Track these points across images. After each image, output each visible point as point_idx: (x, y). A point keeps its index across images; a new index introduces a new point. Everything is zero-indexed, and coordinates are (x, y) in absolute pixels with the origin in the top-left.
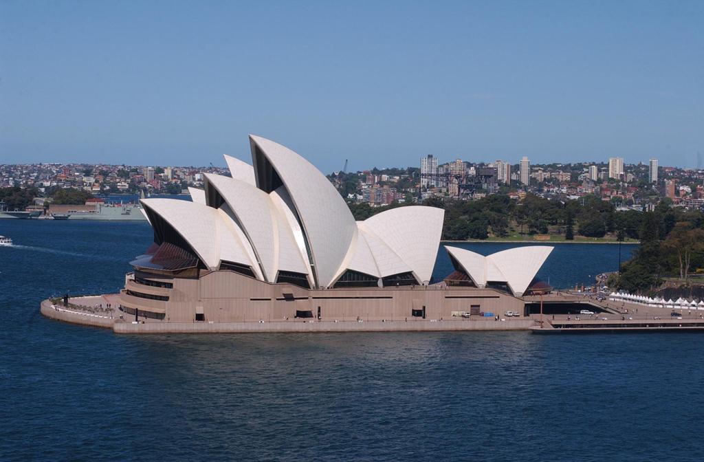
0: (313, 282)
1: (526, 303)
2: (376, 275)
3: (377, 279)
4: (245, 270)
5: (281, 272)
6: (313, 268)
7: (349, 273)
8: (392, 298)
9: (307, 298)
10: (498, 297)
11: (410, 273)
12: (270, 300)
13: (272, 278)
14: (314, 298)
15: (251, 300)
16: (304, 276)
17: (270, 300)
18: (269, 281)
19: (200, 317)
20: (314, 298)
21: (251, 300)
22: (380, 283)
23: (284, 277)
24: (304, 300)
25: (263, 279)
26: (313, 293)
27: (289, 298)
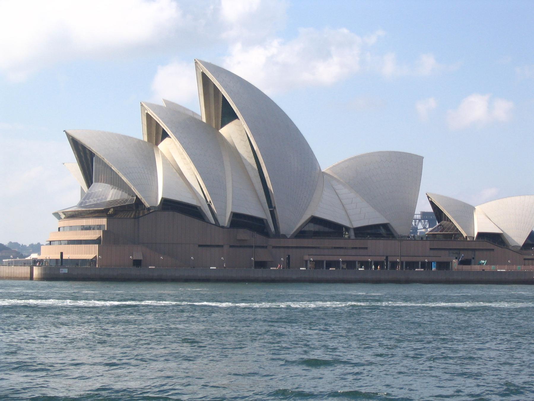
0: (273, 229)
2: (347, 224)
3: (347, 229)
4: (191, 211)
5: (235, 215)
6: (273, 214)
7: (314, 220)
8: (366, 248)
9: (266, 247)
10: (493, 250)
11: (386, 226)
12: (222, 246)
13: (225, 220)
14: (274, 247)
15: (200, 246)
18: (221, 224)
19: (137, 263)
21: (200, 246)
22: (352, 233)
23: (239, 220)
25: (213, 222)
26: (273, 242)
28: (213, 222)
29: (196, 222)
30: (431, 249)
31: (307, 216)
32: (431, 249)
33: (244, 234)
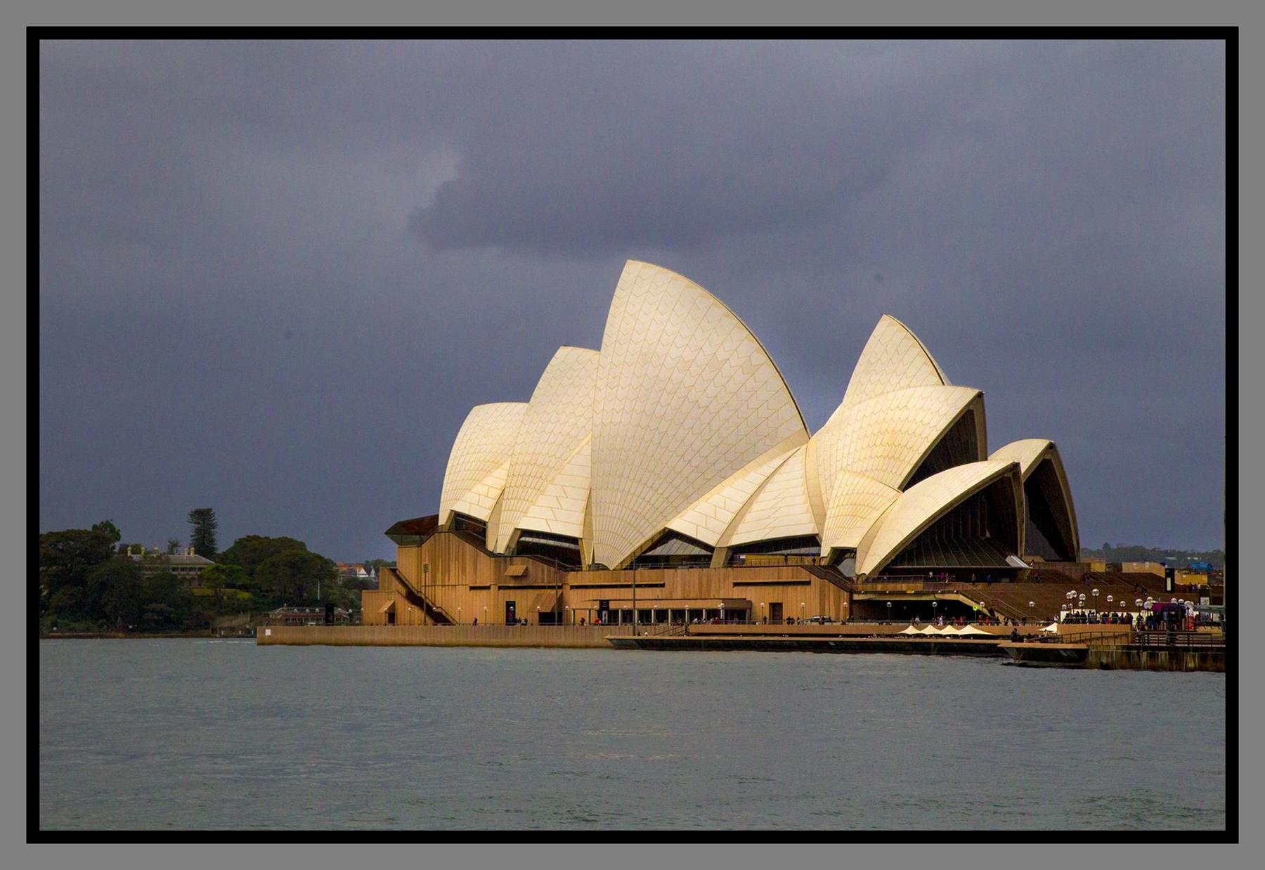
1: (856, 597)
2: (711, 541)
3: (710, 548)
8: (663, 585)
9: (560, 587)
10: (808, 583)
12: (488, 588)
14: (572, 587)
15: (472, 588)
16: (574, 540)
17: (488, 588)
20: (572, 587)
21: (472, 588)
22: (718, 559)
24: (553, 592)
26: (573, 578)
27: (521, 584)
28: (490, 547)
29: (469, 548)
30: (736, 584)
31: (660, 528)
32: (736, 584)
33: (517, 568)
